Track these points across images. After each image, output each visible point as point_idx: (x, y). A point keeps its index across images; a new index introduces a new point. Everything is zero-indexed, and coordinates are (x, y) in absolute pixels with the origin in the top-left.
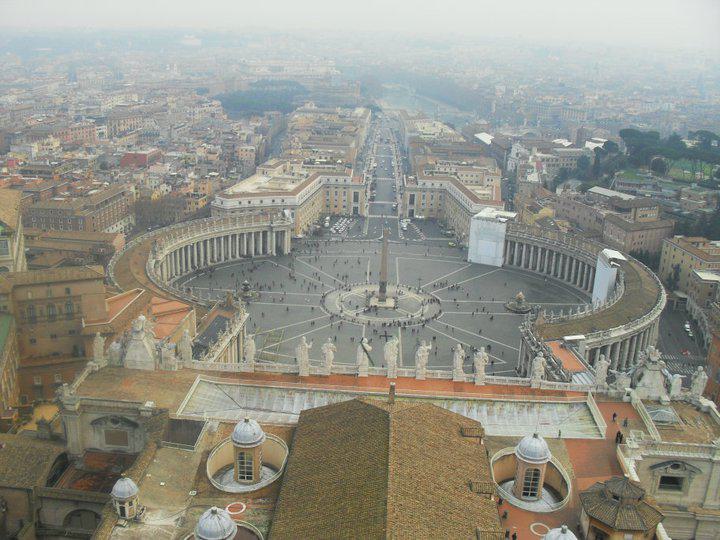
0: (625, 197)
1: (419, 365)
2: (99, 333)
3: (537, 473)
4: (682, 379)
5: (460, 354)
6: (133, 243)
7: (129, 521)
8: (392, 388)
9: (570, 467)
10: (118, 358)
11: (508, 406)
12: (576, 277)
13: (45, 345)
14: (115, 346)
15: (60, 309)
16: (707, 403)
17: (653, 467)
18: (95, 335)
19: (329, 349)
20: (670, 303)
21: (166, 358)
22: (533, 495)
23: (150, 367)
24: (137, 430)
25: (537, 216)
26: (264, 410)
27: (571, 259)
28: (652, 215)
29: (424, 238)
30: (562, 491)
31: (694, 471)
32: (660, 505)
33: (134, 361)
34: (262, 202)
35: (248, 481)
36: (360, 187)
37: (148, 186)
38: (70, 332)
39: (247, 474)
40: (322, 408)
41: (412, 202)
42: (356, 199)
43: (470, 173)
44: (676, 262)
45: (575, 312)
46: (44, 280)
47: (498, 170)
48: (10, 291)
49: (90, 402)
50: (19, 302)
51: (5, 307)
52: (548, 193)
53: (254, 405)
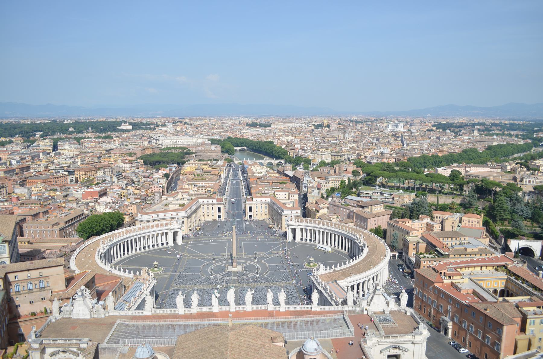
1: (247, 303)
2: (56, 299)
5: (270, 296)
6: (87, 243)
8: (230, 317)
10: (68, 313)
16: (410, 311)
19: (195, 298)
21: (98, 311)
23: (88, 317)
25: (318, 214)
28: (380, 208)
34: (165, 215)
36: (221, 204)
43: (281, 193)
45: (341, 265)
48: (3, 276)
52: (324, 200)
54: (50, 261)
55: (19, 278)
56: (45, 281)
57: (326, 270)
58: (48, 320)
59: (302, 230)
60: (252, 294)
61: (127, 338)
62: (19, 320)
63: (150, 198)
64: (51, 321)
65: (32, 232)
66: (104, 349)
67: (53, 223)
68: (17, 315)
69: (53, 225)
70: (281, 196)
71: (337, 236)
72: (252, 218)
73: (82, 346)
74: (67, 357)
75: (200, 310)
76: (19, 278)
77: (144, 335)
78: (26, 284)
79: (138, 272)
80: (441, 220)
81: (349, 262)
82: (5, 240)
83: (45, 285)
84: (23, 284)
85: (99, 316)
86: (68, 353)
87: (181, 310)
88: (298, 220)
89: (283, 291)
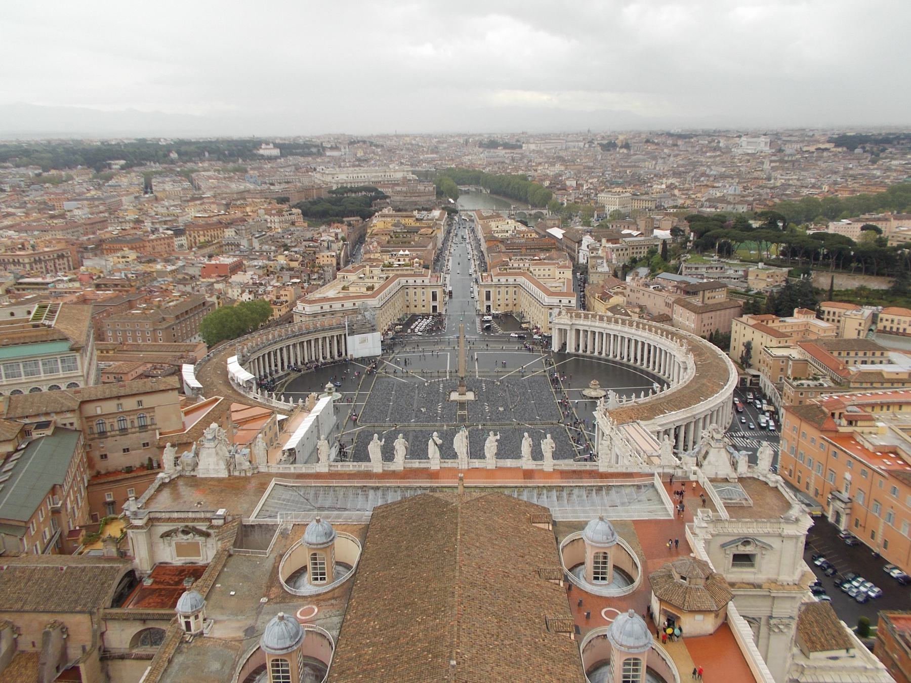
0: (693, 281)
2: (168, 444)
3: (605, 558)
4: (749, 456)
5: (526, 445)
7: (195, 636)
8: (461, 479)
9: (639, 549)
10: (190, 468)
11: (576, 491)
12: (648, 361)
13: (117, 460)
14: (187, 456)
15: (132, 422)
17: (723, 546)
18: (165, 447)
19: (400, 445)
20: (742, 381)
21: (240, 464)
22: (603, 579)
23: (224, 474)
24: (209, 540)
26: (339, 509)
27: (643, 343)
29: (501, 332)
30: (634, 577)
31: (766, 547)
32: (732, 585)
33: (208, 470)
35: (323, 582)
37: (230, 295)
39: (319, 576)
40: (394, 503)
41: (488, 298)
42: (434, 298)
44: (745, 340)
45: (646, 395)
46: (115, 394)
47: (568, 262)
48: (76, 408)
49: (158, 515)
50: (87, 418)
51: (72, 424)
53: (327, 504)
57: (621, 402)
59: (578, 331)
60: (497, 441)
61: (289, 510)
63: (315, 276)
66: (252, 526)
70: (542, 272)
71: (640, 344)
72: (493, 311)
73: (215, 522)
74: (190, 541)
75: (409, 465)
77: (318, 505)
79: (300, 400)
80: (836, 318)
81: (662, 390)
84: (111, 420)
85: (243, 474)
86: (191, 534)
87: (376, 464)
88: (571, 314)
89: (549, 436)
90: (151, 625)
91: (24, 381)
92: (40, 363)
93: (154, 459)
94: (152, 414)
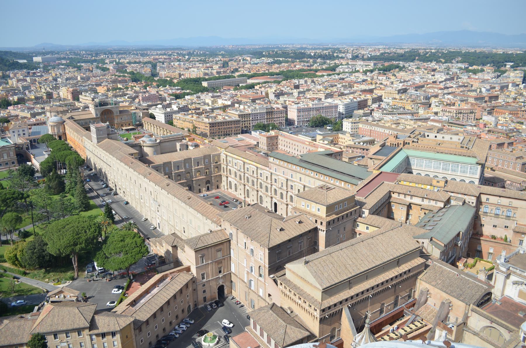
38: (505, 227)
48: (477, 195)
51: (473, 203)
54: (522, 194)
55: (490, 201)
56: (513, 211)
58: (517, 250)
62: (481, 238)
64: (519, 251)
65: (495, 160)
67: (517, 156)
68: (480, 233)
69: (517, 158)
76: (490, 201)
78: (495, 208)
82: (479, 162)
83: (511, 214)
84: (492, 207)
90: (494, 325)
91: (450, 173)
92: (460, 166)
93: (508, 237)
94: (515, 211)
